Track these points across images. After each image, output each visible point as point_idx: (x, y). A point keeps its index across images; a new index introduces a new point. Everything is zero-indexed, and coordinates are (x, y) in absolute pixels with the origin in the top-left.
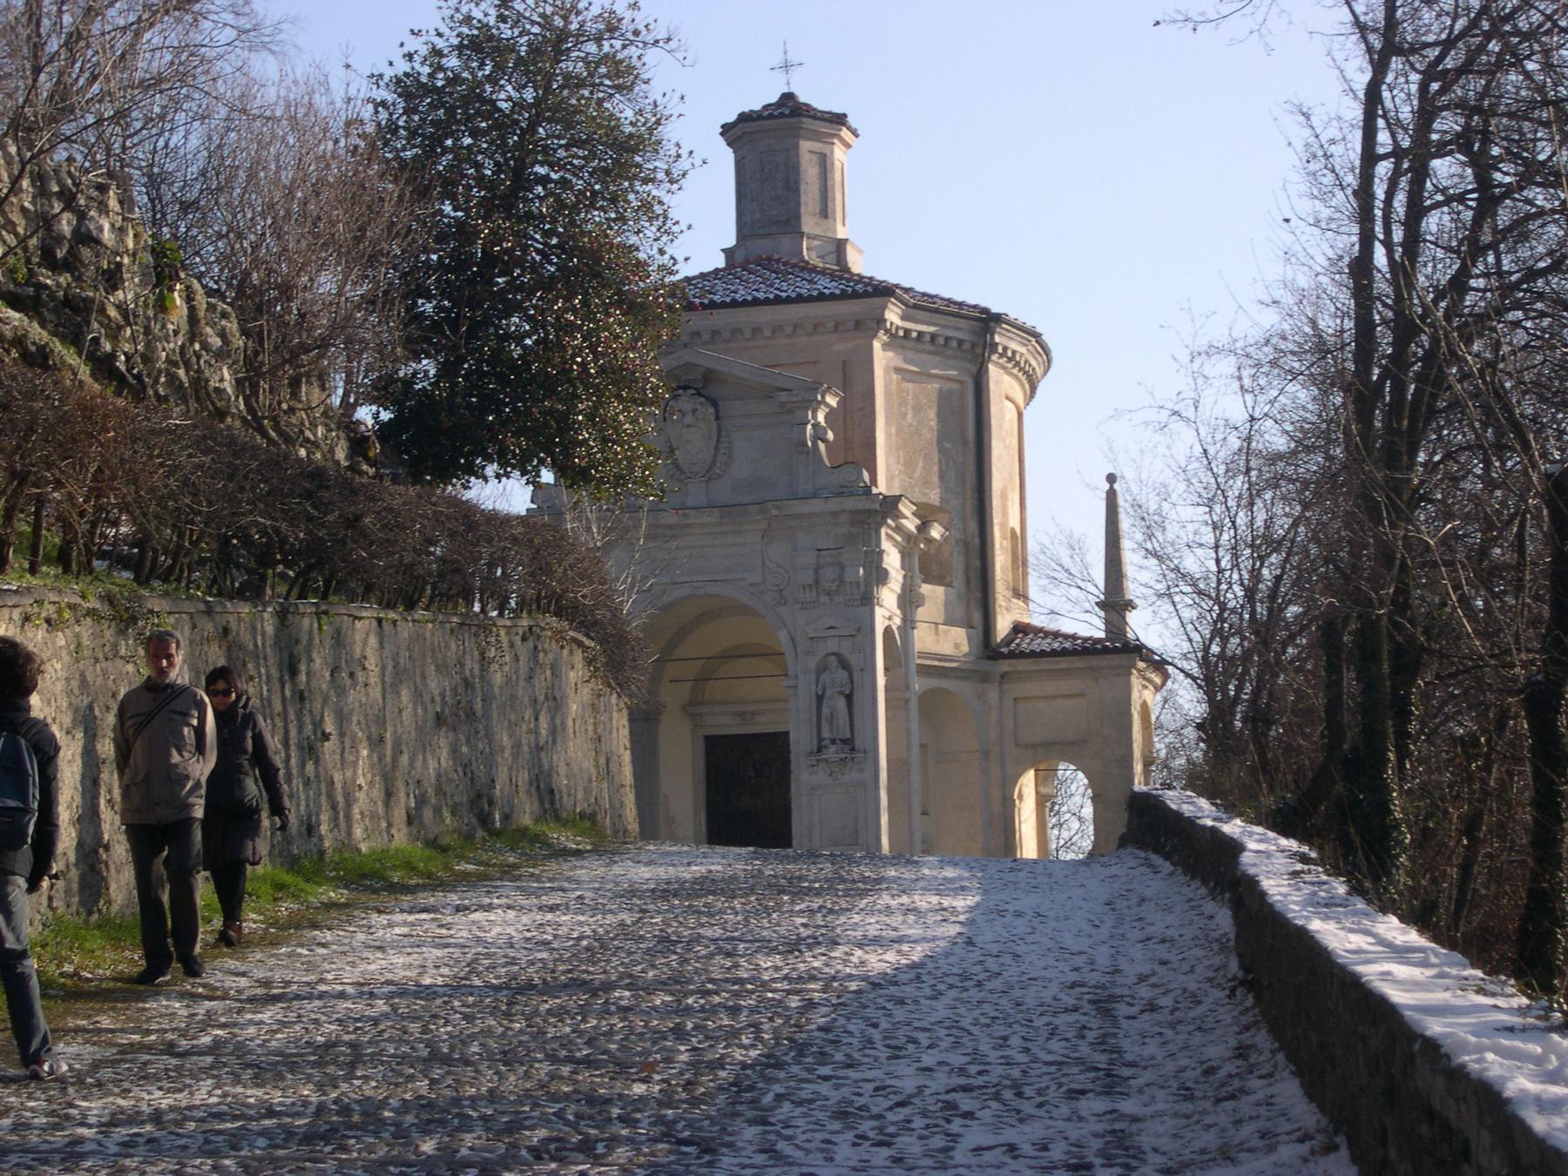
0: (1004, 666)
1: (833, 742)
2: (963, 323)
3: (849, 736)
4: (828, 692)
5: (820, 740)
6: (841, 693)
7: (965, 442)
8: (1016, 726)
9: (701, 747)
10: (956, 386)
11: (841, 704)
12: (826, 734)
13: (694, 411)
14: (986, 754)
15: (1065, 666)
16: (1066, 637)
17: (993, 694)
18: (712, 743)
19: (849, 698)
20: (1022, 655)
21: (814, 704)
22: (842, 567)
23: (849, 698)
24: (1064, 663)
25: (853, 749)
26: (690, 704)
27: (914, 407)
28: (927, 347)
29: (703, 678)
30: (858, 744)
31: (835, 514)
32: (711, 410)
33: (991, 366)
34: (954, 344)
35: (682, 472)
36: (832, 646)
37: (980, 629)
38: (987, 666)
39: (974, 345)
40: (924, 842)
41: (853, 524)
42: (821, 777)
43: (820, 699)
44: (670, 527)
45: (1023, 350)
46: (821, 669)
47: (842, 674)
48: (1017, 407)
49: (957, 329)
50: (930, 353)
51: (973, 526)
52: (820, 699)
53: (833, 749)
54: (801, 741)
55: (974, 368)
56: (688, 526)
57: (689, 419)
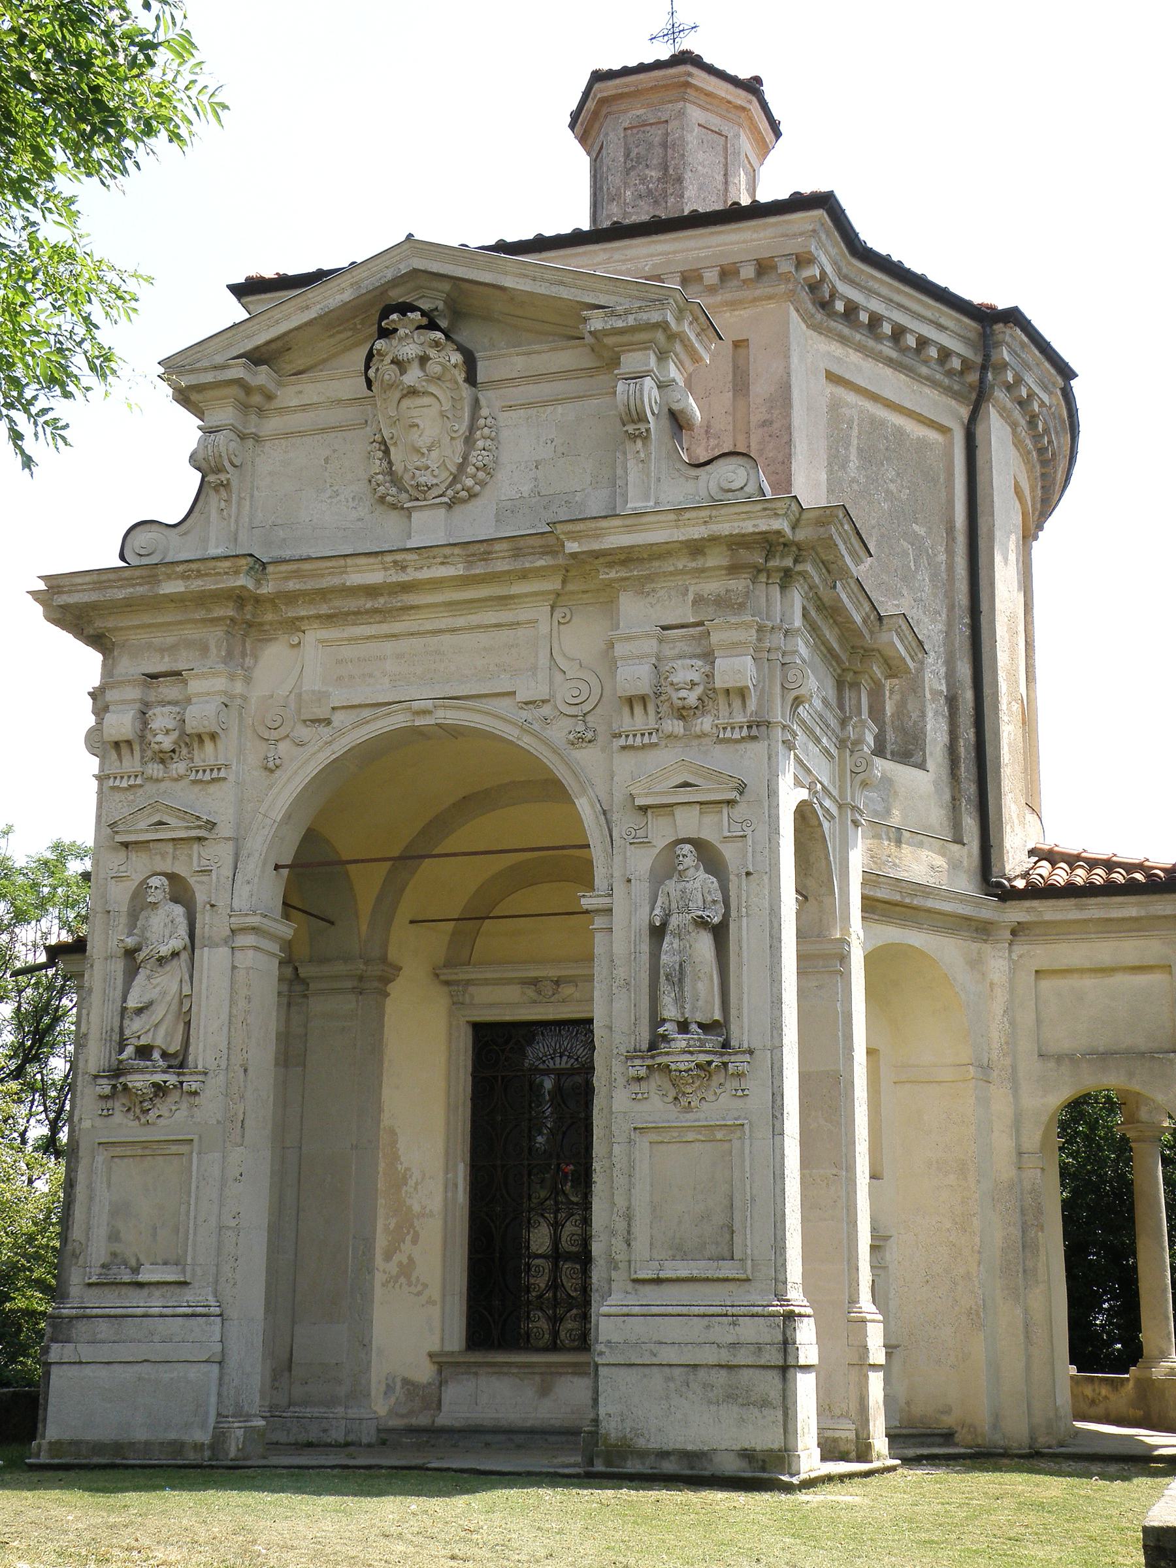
0: (1016, 913)
1: (683, 1027)
2: (949, 317)
3: (717, 1016)
4: (674, 921)
5: (657, 1021)
6: (701, 923)
7: (950, 529)
8: (1039, 1022)
9: (465, 1040)
10: (933, 435)
11: (704, 945)
12: (670, 1011)
13: (423, 360)
14: (985, 1069)
15: (1133, 912)
16: (1130, 868)
17: (997, 963)
18: (479, 1028)
19: (720, 933)
20: (1050, 892)
21: (645, 948)
22: (708, 656)
23: (720, 933)
24: (1129, 908)
25: (726, 1045)
26: (448, 964)
27: (860, 450)
28: (887, 349)
29: (476, 916)
30: (740, 1034)
31: (696, 548)
32: (456, 358)
33: (993, 413)
34: (933, 352)
35: (402, 489)
36: (689, 823)
37: (974, 845)
38: (990, 910)
39: (966, 364)
40: (874, 1229)
41: (733, 569)
42: (655, 1105)
43: (658, 932)
44: (371, 591)
45: (1045, 397)
46: (667, 868)
47: (701, 882)
48: (1025, 515)
49: (941, 327)
50: (889, 362)
51: (964, 670)
52: (658, 932)
53: (681, 1041)
54: (616, 1019)
55: (965, 412)
56: (407, 587)
57: (413, 376)
